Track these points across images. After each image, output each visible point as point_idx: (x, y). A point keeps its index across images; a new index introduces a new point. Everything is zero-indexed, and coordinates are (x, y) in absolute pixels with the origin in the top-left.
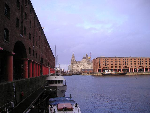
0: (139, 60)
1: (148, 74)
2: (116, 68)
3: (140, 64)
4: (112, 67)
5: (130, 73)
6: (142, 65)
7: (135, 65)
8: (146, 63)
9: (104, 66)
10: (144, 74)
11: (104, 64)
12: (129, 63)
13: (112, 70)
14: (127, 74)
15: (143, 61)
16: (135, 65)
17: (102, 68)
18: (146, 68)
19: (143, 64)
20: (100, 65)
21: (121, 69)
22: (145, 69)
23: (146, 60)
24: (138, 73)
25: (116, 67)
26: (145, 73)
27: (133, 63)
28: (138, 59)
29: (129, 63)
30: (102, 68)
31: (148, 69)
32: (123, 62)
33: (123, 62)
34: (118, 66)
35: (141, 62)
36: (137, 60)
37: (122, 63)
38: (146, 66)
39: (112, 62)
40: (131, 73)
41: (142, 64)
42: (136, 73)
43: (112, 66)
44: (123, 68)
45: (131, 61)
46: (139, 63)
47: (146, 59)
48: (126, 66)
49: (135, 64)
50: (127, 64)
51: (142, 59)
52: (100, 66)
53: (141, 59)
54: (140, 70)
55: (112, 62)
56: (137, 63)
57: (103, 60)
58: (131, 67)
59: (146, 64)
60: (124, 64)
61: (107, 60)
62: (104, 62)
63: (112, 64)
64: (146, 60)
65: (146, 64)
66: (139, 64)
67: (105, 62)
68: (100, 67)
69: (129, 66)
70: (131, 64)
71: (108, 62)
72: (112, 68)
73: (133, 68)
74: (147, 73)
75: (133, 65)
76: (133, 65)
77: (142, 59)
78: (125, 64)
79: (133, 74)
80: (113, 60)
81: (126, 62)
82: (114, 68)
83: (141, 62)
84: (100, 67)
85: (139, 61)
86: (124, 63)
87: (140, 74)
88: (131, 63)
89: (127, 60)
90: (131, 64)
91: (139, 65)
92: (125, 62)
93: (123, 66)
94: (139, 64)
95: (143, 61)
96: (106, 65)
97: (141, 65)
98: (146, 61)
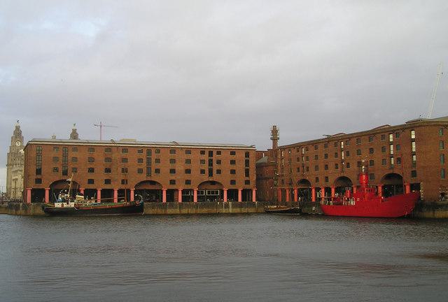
0: (206, 157)
1: (238, 210)
2: (108, 187)
3: (207, 172)
4: (91, 181)
5: (164, 206)
6: (216, 177)
7: (187, 177)
8: (233, 167)
9: (59, 177)
10: (224, 211)
12: (165, 167)
13: (90, 193)
14: (145, 211)
15: (219, 162)
16: (187, 177)
18: (233, 187)
19: (219, 172)
20: (39, 172)
21: (129, 191)
22: (229, 191)
23: (233, 157)
24: (196, 206)
25: (108, 182)
26: (227, 206)
27: (180, 167)
28: (203, 153)
29: (165, 167)
31: (240, 193)
32: (140, 160)
33: (140, 160)
34: (117, 176)
35: (211, 164)
36: (196, 157)
37: (133, 165)
38: (233, 182)
39: (91, 160)
40: (172, 206)
41: (215, 172)
42: (187, 206)
43: (91, 176)
44: (141, 188)
45: (173, 161)
46: (206, 167)
47: (233, 153)
48: (149, 179)
49: (188, 171)
50: (153, 170)
51: (219, 153)
52: (39, 177)
53: (215, 153)
54: (208, 197)
55: (91, 160)
56: (196, 167)
57: (54, 154)
58: (173, 182)
59: (233, 172)
60: (140, 171)
61: (72, 154)
62: (56, 159)
63: (91, 170)
64: (233, 157)
65: (233, 172)
66: (203, 172)
67: (61, 158)
68: (39, 181)
69: (164, 180)
70: (173, 171)
71: (75, 159)
72: (91, 187)
73: (181, 187)
74: (234, 206)
75: (180, 177)
76: (180, 177)
77: (219, 153)
79: (177, 211)
80: (95, 155)
82: (100, 186)
83: (211, 164)
84: (39, 181)
85: (203, 162)
86: (144, 166)
87: (205, 210)
88: (171, 166)
89: (154, 156)
90: (173, 171)
91: (206, 178)
93: (134, 179)
94: (203, 172)
95: (219, 162)
96: (65, 173)
97: (211, 173)
98: (233, 162)
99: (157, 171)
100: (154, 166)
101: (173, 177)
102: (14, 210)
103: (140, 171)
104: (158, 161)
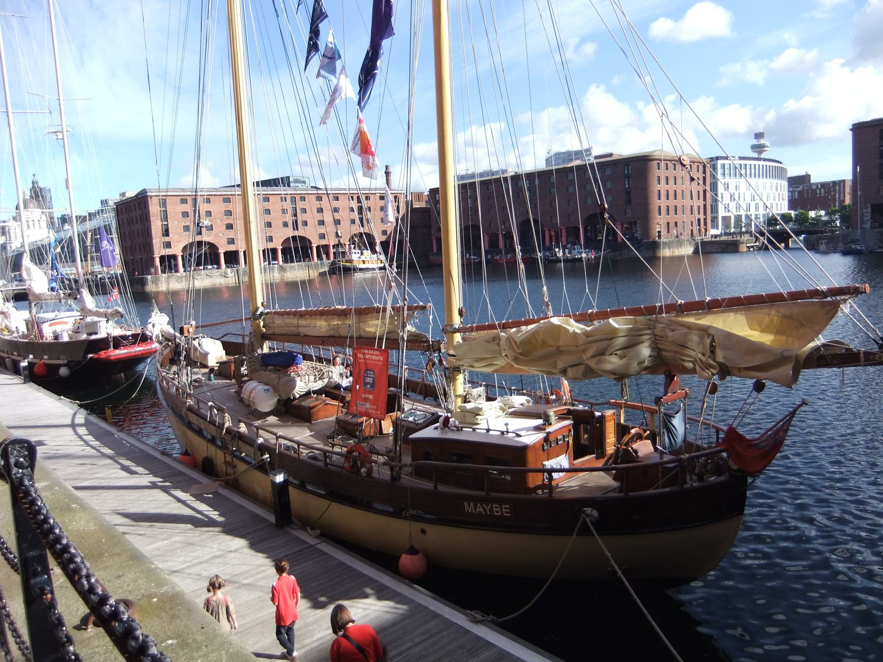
11: (186, 228)
12: (312, 217)
17: (177, 250)
27: (328, 217)
29: (312, 217)
30: (177, 250)
52: (167, 239)
58: (322, 236)
60: (285, 225)
62: (185, 214)
69: (311, 234)
71: (209, 214)
78: (290, 225)
81: (298, 211)
84: (168, 245)
90: (321, 223)
92: (290, 211)
99: (305, 223)
100: (301, 217)
101: (322, 230)
102: (140, 287)
103: (285, 225)
104: (304, 211)
